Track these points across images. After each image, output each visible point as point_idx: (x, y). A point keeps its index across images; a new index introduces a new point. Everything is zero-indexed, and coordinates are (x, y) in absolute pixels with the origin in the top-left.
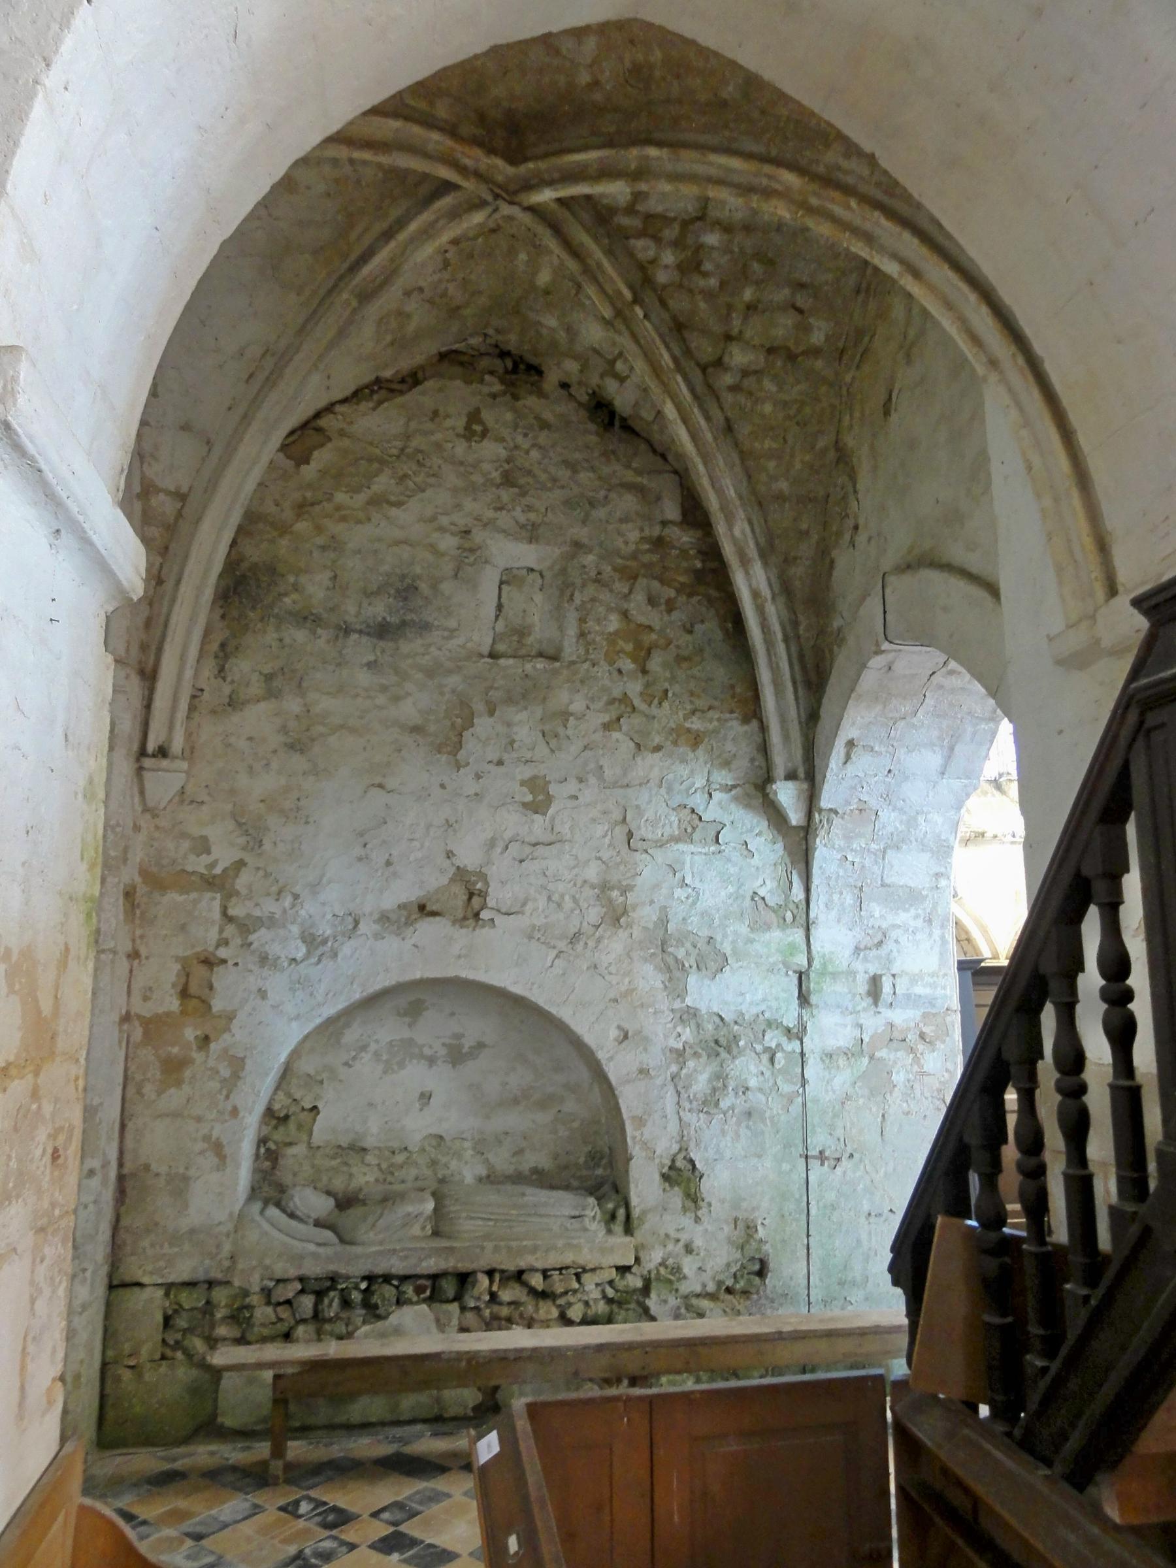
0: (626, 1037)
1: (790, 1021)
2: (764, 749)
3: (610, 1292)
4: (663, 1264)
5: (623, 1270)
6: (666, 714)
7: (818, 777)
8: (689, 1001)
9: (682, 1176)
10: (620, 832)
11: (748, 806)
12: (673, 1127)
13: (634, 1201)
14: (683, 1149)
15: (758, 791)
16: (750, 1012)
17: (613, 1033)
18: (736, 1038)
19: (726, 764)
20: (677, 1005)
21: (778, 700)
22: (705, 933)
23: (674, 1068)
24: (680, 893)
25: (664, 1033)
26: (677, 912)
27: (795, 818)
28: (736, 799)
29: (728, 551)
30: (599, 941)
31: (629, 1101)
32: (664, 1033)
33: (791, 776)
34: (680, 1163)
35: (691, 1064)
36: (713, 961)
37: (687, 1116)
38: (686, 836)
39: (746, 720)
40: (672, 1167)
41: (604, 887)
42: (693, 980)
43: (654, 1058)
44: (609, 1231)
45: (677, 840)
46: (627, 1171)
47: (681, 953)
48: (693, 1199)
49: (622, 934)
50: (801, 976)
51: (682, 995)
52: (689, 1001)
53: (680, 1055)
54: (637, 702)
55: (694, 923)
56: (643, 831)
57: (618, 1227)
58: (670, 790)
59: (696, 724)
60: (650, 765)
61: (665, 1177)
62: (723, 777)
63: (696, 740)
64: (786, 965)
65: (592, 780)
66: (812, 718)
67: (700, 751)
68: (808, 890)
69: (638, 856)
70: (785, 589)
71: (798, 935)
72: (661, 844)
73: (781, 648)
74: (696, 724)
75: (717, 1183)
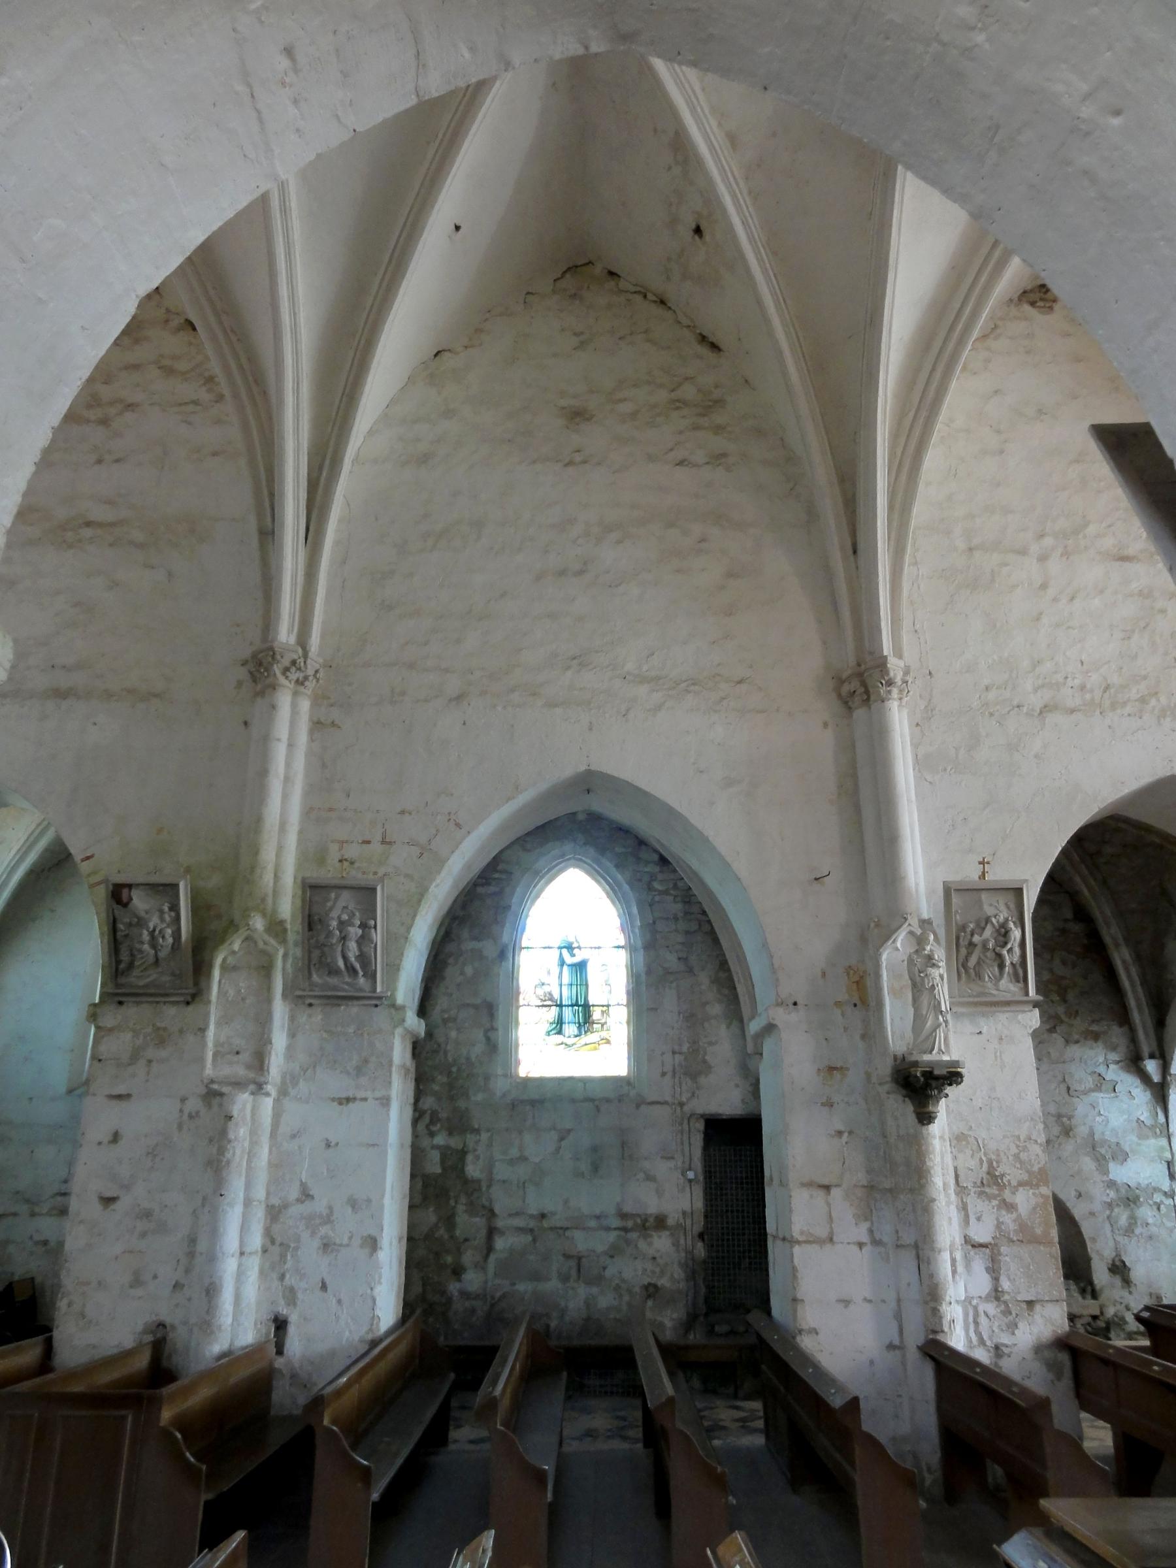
0: (1080, 1195)
1: (1166, 1188)
2: (1133, 1040)
3: (1089, 1329)
4: (1115, 1315)
5: (1095, 1318)
6: (1079, 1024)
7: (1168, 1057)
8: (1111, 1176)
9: (1119, 1269)
10: (1063, 1088)
11: (1128, 1072)
12: (1111, 1243)
13: (1096, 1282)
14: (1118, 1255)
15: (1134, 1063)
16: (1144, 1183)
17: (1073, 1193)
18: (1138, 1197)
19: (1114, 1048)
20: (1105, 1178)
21: (1140, 1017)
22: (1114, 1140)
23: (1108, 1212)
24: (1098, 1119)
25: (1101, 1195)
26: (1098, 1130)
27: (1156, 1078)
28: (1122, 1068)
29: (1108, 940)
30: (1060, 1144)
31: (1087, 1230)
32: (1101, 1195)
33: (1152, 1056)
34: (1118, 1263)
35: (1116, 1210)
36: (1121, 1156)
37: (1119, 1238)
38: (1098, 1088)
39: (1121, 1025)
40: (1114, 1264)
41: (1059, 1116)
42: (1112, 1166)
43: (1097, 1206)
44: (1084, 1298)
45: (1093, 1091)
46: (1089, 1267)
47: (1103, 1151)
48: (1127, 1282)
49: (1072, 1141)
50: (1169, 1163)
51: (1107, 1173)
52: (1111, 1176)
53: (1110, 1205)
54: (1063, 1017)
55: (1108, 1135)
56: (1075, 1086)
57: (1089, 1297)
58: (1086, 1063)
59: (1095, 1028)
60: (1074, 1051)
61: (1110, 1270)
62: (1113, 1056)
63: (1096, 1037)
64: (1161, 1158)
65: (1045, 1060)
66: (1160, 1024)
67: (1100, 1043)
68: (1167, 1117)
69: (1075, 1100)
70: (1138, 958)
71: (1164, 1142)
72: (1085, 1093)
73: (1139, 989)
74: (1095, 1028)
75: (1138, 1273)
